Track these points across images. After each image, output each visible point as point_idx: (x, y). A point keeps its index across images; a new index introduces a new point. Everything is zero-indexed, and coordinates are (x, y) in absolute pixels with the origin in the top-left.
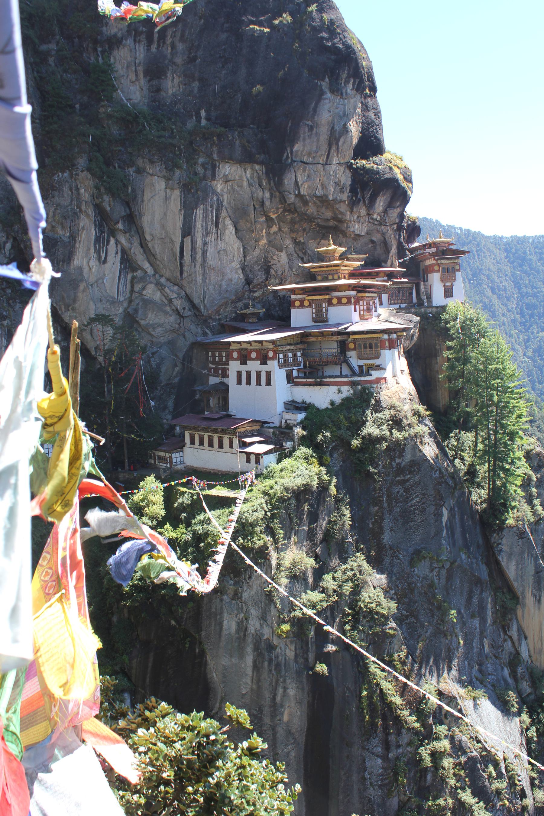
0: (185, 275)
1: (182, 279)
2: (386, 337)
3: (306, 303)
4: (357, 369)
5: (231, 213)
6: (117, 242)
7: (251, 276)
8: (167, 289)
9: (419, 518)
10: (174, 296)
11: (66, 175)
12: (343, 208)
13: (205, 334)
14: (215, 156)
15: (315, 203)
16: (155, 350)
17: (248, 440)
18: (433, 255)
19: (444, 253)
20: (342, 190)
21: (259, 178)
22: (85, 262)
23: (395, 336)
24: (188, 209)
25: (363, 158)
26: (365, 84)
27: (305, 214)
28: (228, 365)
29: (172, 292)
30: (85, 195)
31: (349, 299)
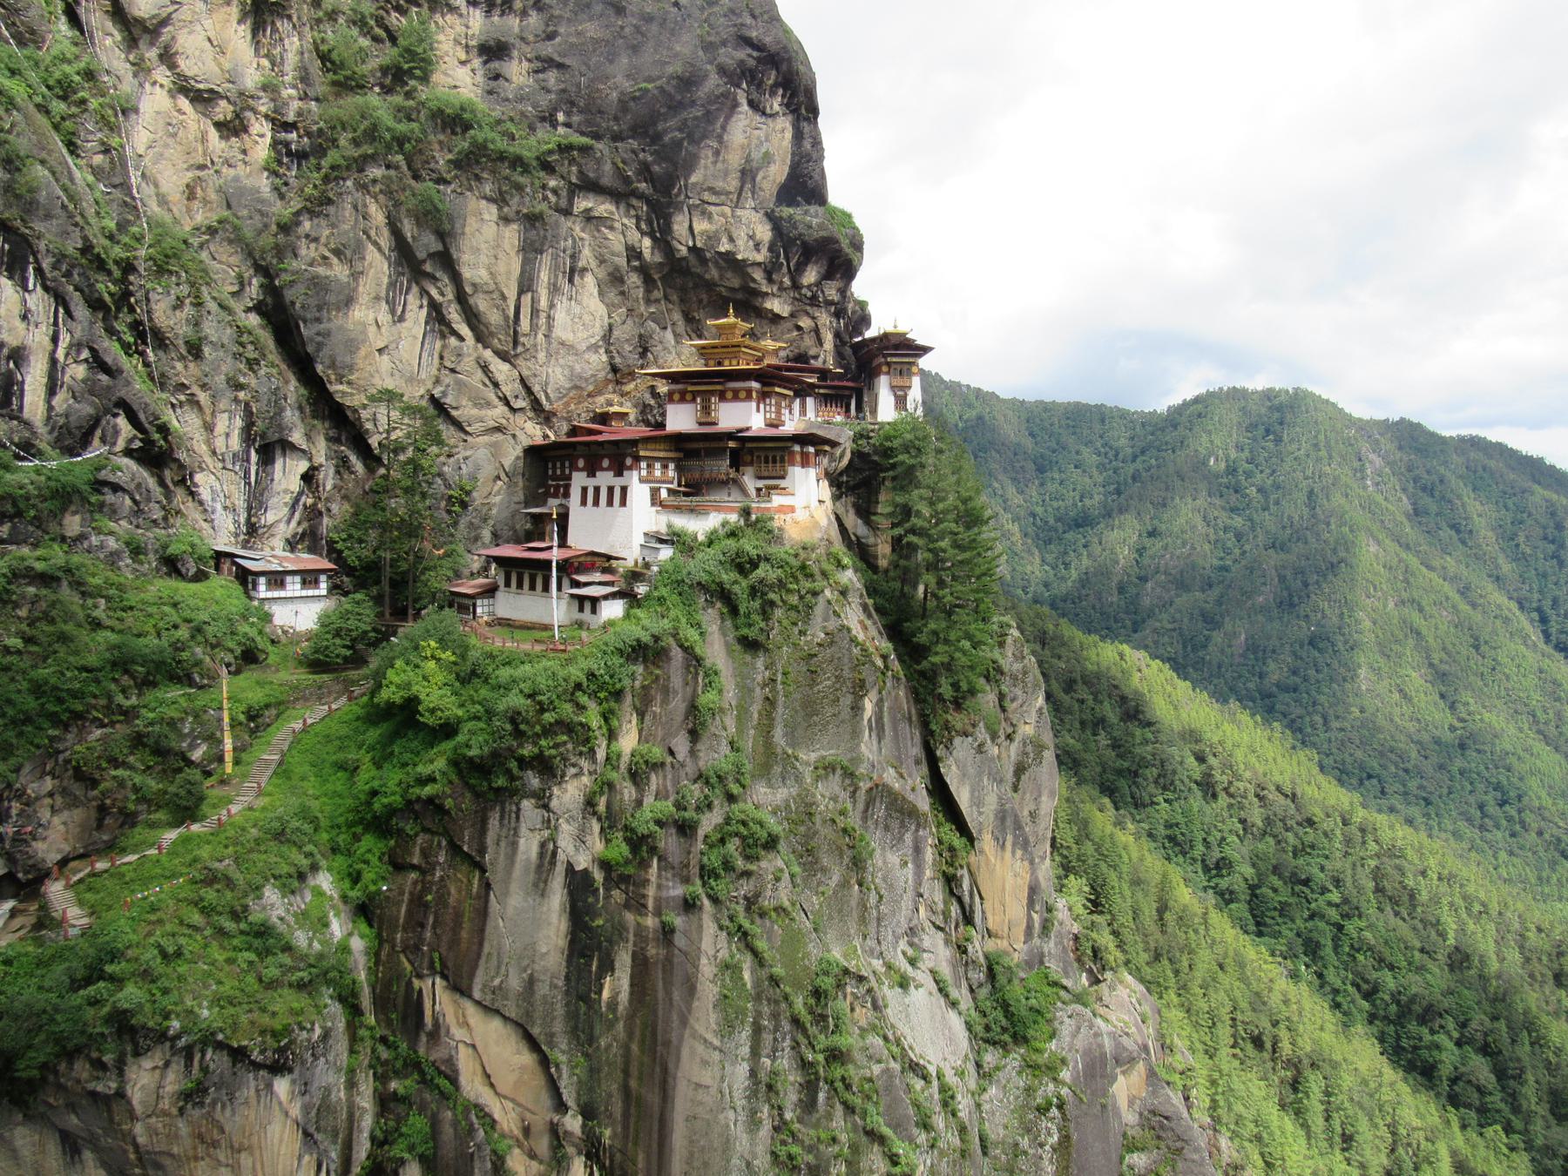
0: (520, 349)
1: (516, 356)
2: (797, 448)
3: (689, 397)
4: (753, 493)
5: (593, 264)
6: (424, 292)
7: (618, 360)
8: (492, 368)
9: (829, 711)
10: (500, 378)
11: (349, 183)
12: (758, 275)
13: (546, 436)
14: (574, 180)
15: (716, 264)
16: (468, 453)
17: (582, 578)
18: (881, 349)
19: (897, 347)
20: (757, 247)
21: (638, 218)
22: (371, 317)
23: (811, 449)
24: (530, 250)
25: (789, 205)
26: (801, 103)
27: (700, 277)
28: (569, 478)
29: (501, 369)
30: (378, 216)
31: (749, 392)
